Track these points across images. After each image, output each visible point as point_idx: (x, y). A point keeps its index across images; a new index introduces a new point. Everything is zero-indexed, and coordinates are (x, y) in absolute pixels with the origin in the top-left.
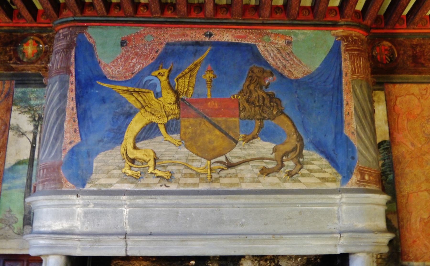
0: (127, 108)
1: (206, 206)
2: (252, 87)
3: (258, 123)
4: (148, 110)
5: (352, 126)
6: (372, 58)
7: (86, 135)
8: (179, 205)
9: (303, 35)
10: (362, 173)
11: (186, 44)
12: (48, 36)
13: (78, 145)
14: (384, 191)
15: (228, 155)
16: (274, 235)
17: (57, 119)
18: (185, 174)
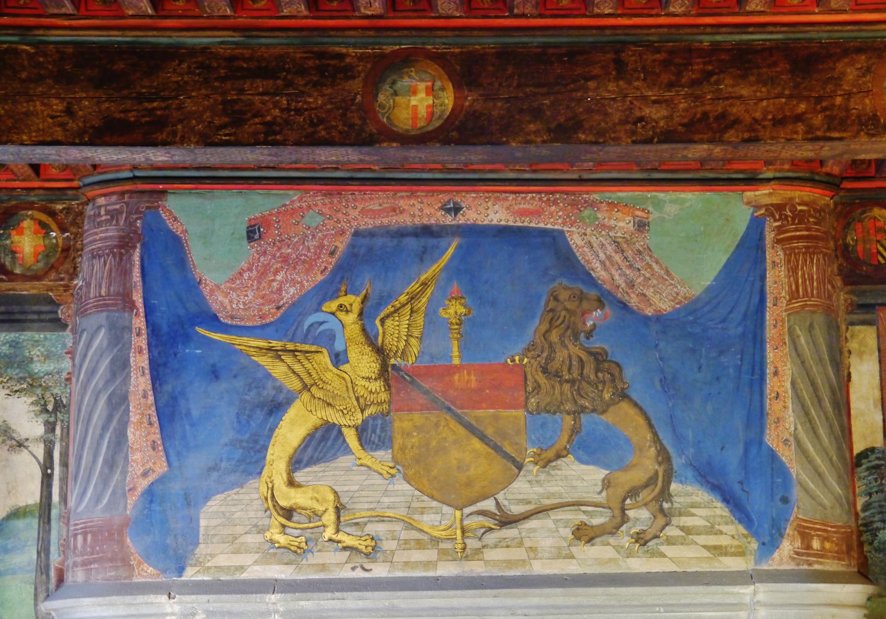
0: (268, 392)
2: (554, 336)
3: (569, 421)
4: (319, 394)
5: (785, 425)
6: (844, 251)
7: (178, 454)
9: (676, 205)
10: (805, 535)
11: (401, 233)
12: (68, 210)
13: (161, 480)
15: (500, 497)
17: (110, 418)
18: (406, 542)
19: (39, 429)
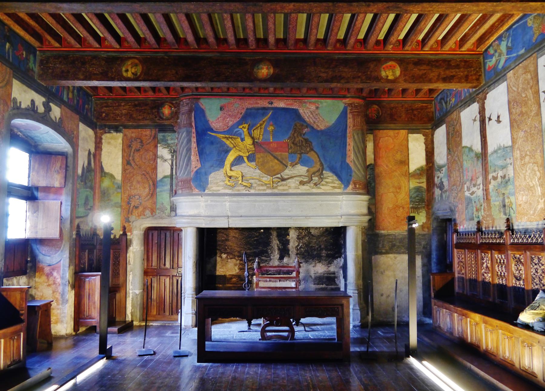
0: (225, 148)
1: (270, 201)
2: (296, 135)
3: (299, 156)
4: (238, 148)
5: (351, 157)
6: (366, 116)
8: (255, 201)
9: (326, 103)
10: (355, 184)
11: (258, 109)
12: (176, 103)
13: (199, 169)
14: (368, 193)
17: (187, 153)
19: (170, 157)
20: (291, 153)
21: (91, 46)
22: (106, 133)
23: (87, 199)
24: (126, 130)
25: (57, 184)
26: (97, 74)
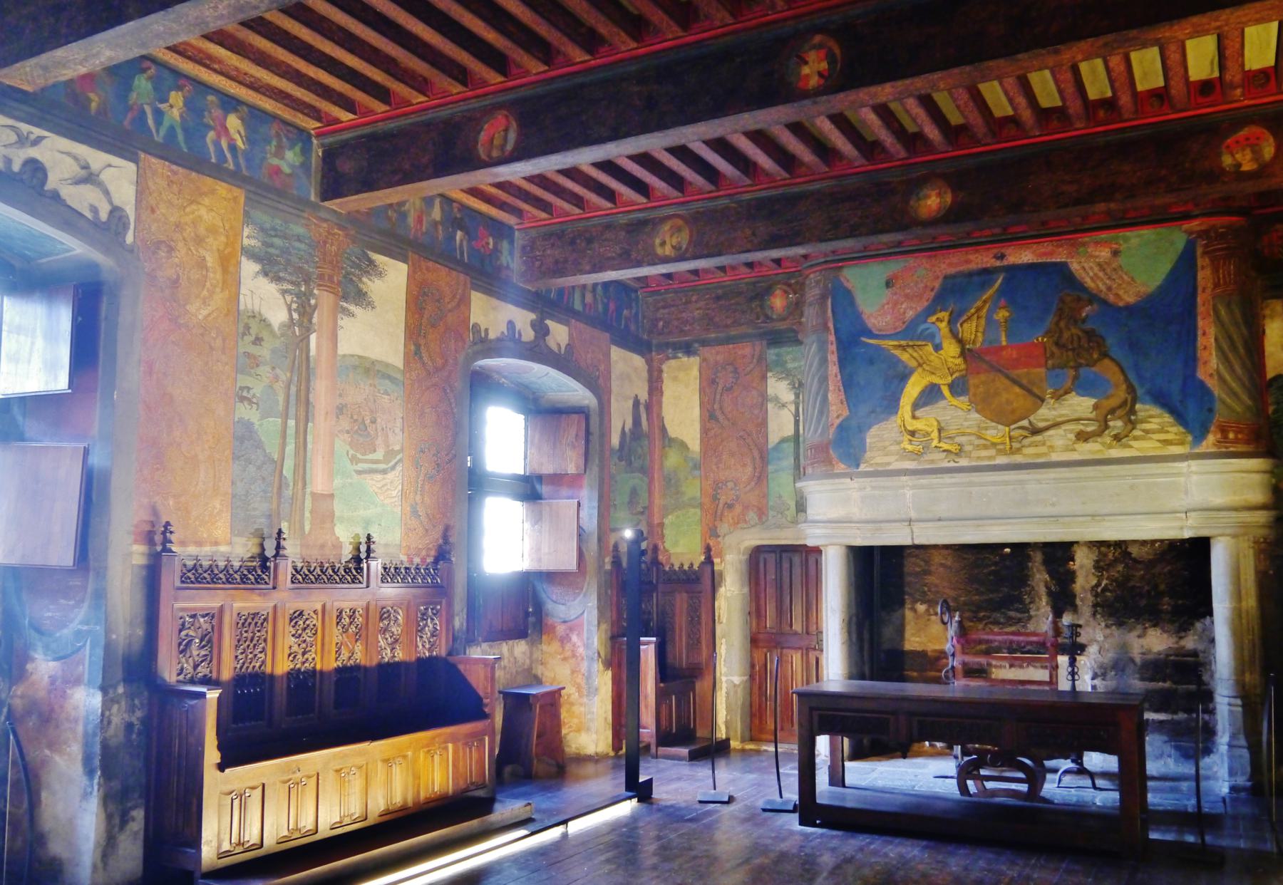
0: (900, 368)
1: (1006, 483)
2: (1062, 324)
3: (1072, 372)
8: (971, 484)
9: (1137, 240)
10: (1223, 430)
11: (970, 274)
13: (847, 419)
16: (1093, 516)
17: (820, 388)
19: (792, 397)
20: (1054, 367)
21: (599, 208)
22: (668, 358)
23: (634, 492)
24: (706, 349)
25: (571, 469)
26: (613, 258)
